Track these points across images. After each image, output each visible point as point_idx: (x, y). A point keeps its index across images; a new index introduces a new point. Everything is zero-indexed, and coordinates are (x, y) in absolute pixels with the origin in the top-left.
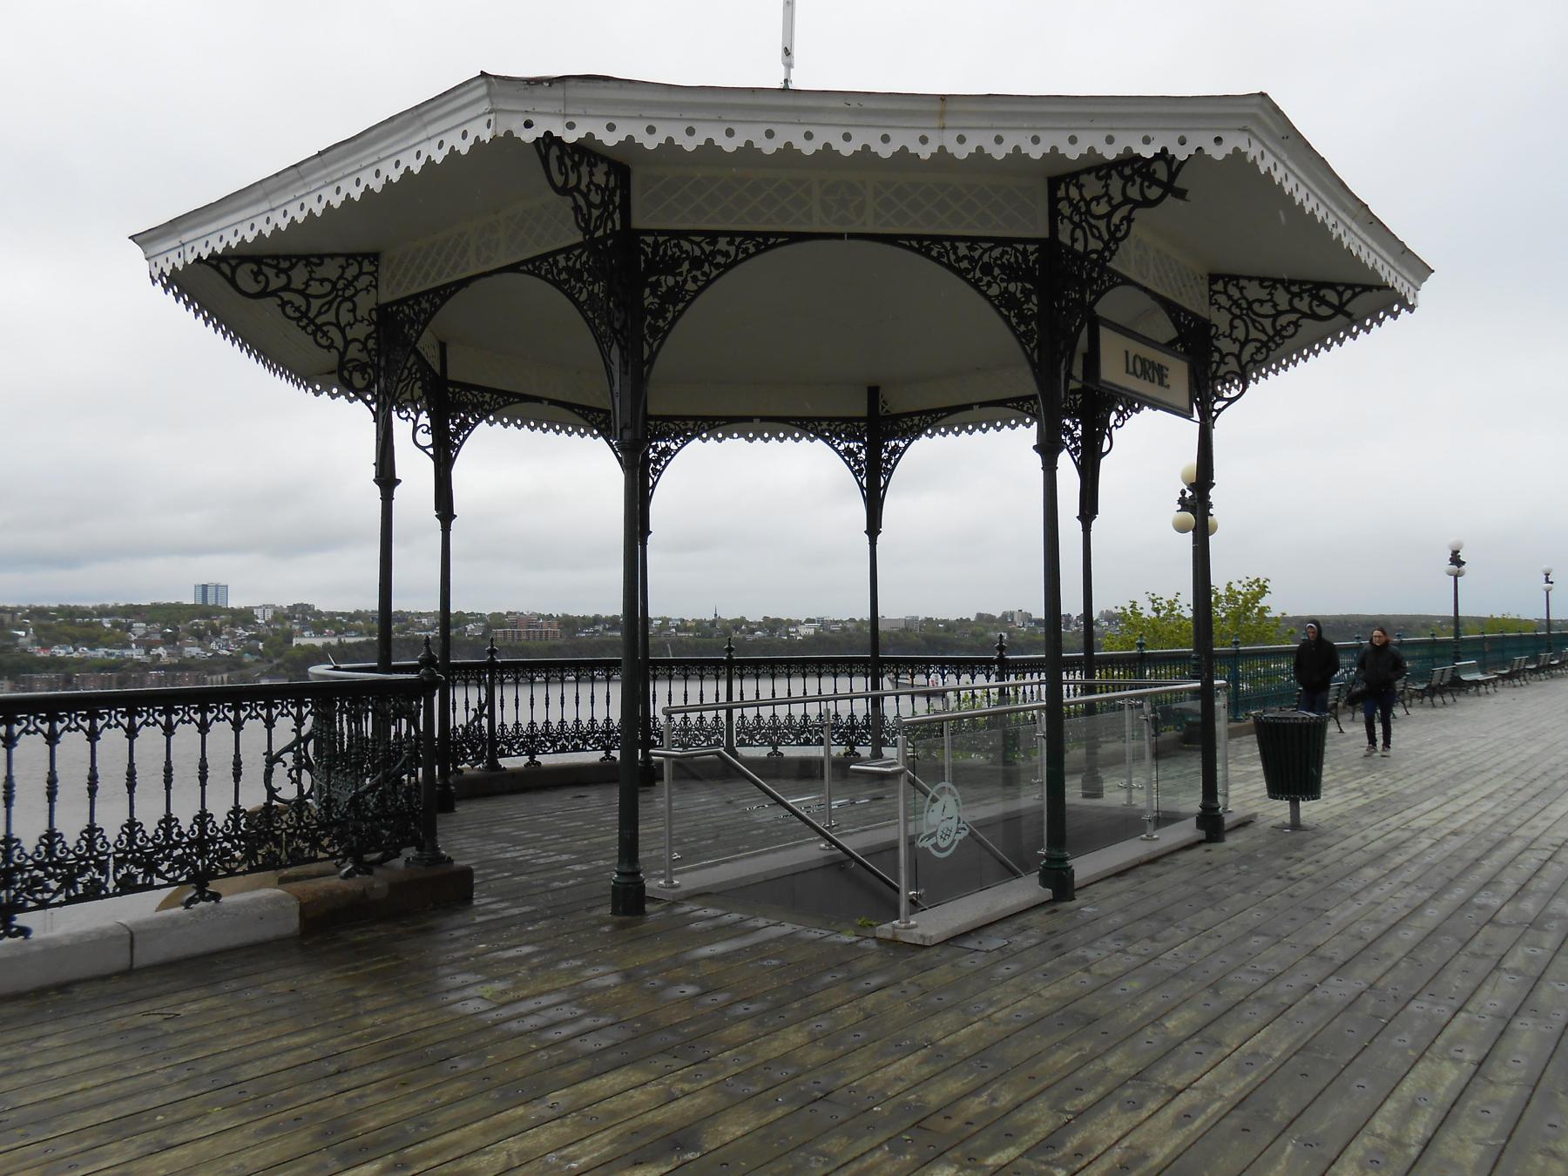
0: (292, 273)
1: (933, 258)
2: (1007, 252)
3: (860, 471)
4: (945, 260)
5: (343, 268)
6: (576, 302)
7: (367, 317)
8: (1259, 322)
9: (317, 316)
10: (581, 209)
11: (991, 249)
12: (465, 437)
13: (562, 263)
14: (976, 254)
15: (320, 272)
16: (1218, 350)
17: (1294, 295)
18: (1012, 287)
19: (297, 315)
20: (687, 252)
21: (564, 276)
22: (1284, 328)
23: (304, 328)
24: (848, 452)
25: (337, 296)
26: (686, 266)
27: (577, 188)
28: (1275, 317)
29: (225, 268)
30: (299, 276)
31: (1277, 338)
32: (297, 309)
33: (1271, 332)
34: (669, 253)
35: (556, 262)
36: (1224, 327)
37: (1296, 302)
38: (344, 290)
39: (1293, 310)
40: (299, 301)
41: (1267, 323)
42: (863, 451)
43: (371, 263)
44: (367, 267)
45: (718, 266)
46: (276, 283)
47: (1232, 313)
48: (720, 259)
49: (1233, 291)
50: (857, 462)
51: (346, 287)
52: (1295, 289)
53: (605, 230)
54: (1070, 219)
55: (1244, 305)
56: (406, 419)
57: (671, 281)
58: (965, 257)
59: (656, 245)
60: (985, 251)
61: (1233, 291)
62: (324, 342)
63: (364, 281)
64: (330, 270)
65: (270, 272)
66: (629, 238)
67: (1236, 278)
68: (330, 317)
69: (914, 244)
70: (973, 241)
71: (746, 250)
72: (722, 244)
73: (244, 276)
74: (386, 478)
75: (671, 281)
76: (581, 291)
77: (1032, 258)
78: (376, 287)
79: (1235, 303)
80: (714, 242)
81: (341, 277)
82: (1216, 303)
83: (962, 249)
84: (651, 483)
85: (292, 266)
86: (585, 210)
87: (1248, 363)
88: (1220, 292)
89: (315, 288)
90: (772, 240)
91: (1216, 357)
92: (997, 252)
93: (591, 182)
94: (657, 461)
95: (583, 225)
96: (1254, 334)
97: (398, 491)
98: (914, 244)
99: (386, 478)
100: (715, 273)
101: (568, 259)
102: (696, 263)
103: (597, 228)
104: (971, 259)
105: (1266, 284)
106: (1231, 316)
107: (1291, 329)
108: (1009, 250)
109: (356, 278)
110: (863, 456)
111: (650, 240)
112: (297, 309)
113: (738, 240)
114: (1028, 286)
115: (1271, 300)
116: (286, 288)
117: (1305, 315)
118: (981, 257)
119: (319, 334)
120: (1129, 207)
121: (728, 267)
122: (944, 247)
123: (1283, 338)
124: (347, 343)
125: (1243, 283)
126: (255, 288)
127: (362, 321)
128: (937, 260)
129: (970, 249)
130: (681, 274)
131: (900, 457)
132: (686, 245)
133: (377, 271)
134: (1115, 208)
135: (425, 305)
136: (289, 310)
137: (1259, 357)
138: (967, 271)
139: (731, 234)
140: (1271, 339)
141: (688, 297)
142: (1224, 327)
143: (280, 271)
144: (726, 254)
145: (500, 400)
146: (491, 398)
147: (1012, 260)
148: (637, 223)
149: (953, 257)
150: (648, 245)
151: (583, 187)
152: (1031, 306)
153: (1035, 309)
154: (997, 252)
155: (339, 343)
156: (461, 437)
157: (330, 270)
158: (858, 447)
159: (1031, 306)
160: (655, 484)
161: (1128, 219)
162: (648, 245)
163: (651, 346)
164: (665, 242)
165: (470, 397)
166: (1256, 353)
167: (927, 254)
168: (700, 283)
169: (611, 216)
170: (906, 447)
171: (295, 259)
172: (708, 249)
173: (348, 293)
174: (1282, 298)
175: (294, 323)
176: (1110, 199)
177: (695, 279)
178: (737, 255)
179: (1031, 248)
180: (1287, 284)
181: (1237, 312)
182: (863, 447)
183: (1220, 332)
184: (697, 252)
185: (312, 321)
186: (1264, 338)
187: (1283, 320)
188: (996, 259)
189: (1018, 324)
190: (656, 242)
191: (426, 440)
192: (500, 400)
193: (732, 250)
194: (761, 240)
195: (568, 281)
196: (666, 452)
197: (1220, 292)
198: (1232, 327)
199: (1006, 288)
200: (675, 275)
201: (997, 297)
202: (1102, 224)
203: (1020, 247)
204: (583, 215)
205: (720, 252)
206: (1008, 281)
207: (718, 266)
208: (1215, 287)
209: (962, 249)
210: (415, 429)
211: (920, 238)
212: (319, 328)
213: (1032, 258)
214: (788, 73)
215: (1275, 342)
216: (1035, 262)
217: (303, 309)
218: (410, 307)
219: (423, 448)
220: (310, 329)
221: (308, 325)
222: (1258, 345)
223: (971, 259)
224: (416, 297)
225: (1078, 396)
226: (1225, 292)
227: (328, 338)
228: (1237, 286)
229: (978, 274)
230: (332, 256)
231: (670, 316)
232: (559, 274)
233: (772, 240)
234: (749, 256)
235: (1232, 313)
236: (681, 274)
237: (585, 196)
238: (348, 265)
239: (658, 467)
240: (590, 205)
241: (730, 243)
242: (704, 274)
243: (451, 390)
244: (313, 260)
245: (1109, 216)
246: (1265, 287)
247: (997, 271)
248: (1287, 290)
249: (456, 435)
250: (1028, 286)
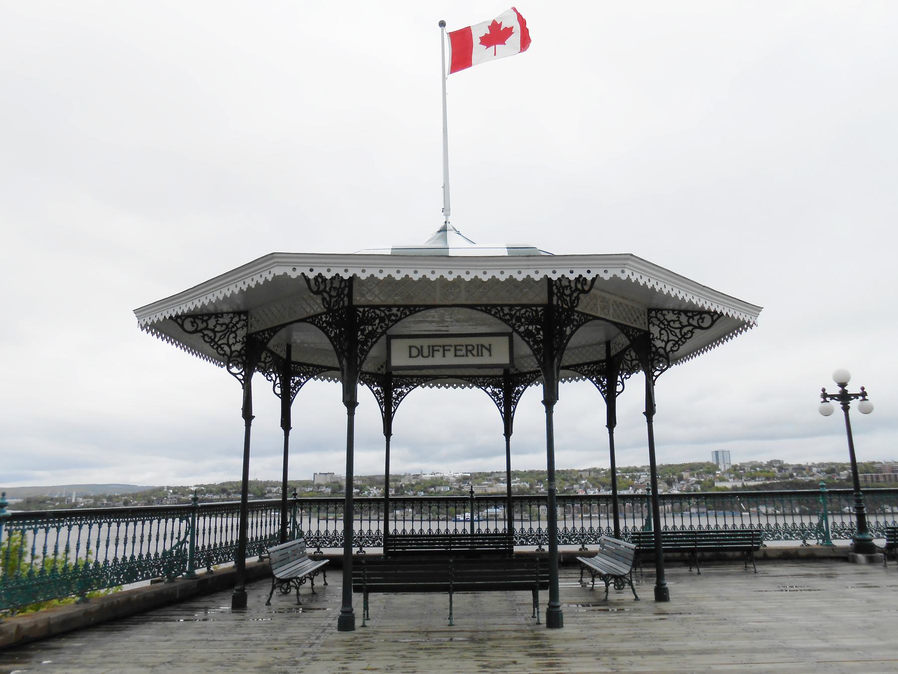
0: (209, 322)
1: (492, 315)
2: (528, 311)
4: (498, 315)
5: (232, 318)
6: (329, 337)
7: (241, 340)
8: (674, 332)
9: (219, 340)
10: (326, 299)
11: (520, 310)
12: (299, 389)
13: (324, 319)
14: (513, 313)
15: (221, 321)
16: (654, 346)
17: (689, 318)
18: (530, 327)
19: (210, 340)
20: (378, 315)
21: (325, 325)
22: (686, 334)
23: (213, 347)
24: (494, 394)
25: (228, 332)
26: (377, 321)
27: (324, 290)
28: (681, 328)
29: (179, 320)
30: (212, 323)
31: (683, 339)
32: (210, 338)
33: (680, 337)
34: (370, 315)
35: (322, 318)
36: (657, 334)
37: (691, 320)
38: (231, 328)
39: (690, 325)
40: (211, 334)
41: (677, 331)
42: (502, 393)
43: (245, 315)
44: (243, 317)
45: (392, 321)
46: (201, 326)
47: (660, 328)
48: (393, 318)
49: (659, 316)
50: (499, 399)
51: (233, 327)
52: (690, 314)
53: (339, 306)
54: (557, 295)
55: (666, 323)
56: (270, 381)
57: (370, 328)
58: (507, 314)
59: (364, 312)
60: (517, 311)
61: (659, 316)
63: (242, 323)
64: (226, 320)
65: (199, 322)
66: (352, 309)
67: (662, 310)
68: (224, 341)
69: (483, 308)
70: (511, 307)
71: (405, 314)
72: (394, 310)
73: (188, 325)
74: (248, 414)
75: (370, 328)
76: (331, 332)
77: (540, 313)
78: (247, 326)
79: (661, 322)
80: (390, 310)
81: (231, 322)
82: (652, 323)
83: (506, 310)
84: (393, 410)
85: (208, 319)
86: (328, 299)
87: (669, 352)
88: (653, 317)
89: (218, 328)
90: (417, 309)
91: (654, 349)
92: (523, 311)
93: (331, 287)
94: (397, 399)
95: (327, 306)
96: (671, 337)
97: (253, 421)
98: (483, 308)
99: (248, 414)
100: (391, 324)
101: (326, 317)
102: (382, 320)
103: (334, 306)
105: (676, 312)
106: (687, 318)
107: (689, 335)
108: (529, 310)
109: (237, 323)
110: (501, 395)
111: (361, 310)
112: (210, 338)
113: (401, 309)
114: (538, 327)
115: (678, 320)
116: (206, 328)
117: (695, 327)
118: (515, 313)
119: (219, 349)
120: (578, 292)
121: (396, 321)
122: (497, 309)
123: (686, 339)
125: (665, 312)
126: (194, 329)
127: (239, 342)
128: (494, 315)
129: (511, 310)
130: (375, 325)
131: (520, 396)
132: (378, 312)
133: (247, 319)
134: (572, 292)
135: (266, 335)
136: (207, 339)
137: (675, 349)
138: (509, 320)
139: (399, 306)
140: (680, 339)
141: (378, 336)
142: (657, 334)
143: (203, 321)
144: (396, 315)
145: (318, 370)
146: (313, 369)
147: (531, 314)
148: (355, 303)
149: (502, 314)
150: (360, 312)
151: (327, 289)
152: (540, 336)
153: (542, 337)
154: (523, 311)
156: (297, 389)
157: (226, 320)
158: (499, 391)
159: (540, 336)
160: (395, 410)
161: (578, 298)
162: (360, 312)
163: (360, 358)
164: (368, 311)
165: (302, 369)
166: (673, 347)
167: (490, 313)
168: (383, 329)
169: (342, 300)
170: (524, 390)
171: (210, 315)
172: (388, 313)
173: (234, 329)
174: (684, 319)
175: (208, 344)
176: (571, 288)
177: (381, 327)
178: (401, 315)
179: (539, 309)
180: (686, 312)
181: (663, 326)
182: (502, 391)
183: (655, 337)
184: (383, 314)
185: (216, 343)
186: (677, 339)
187: (685, 330)
188: (523, 314)
189: (534, 345)
190: (364, 310)
191: (278, 390)
192: (318, 370)
193: (399, 314)
194: (412, 309)
195: (326, 327)
196: (401, 394)
197: (653, 317)
198: (661, 334)
199: (528, 328)
200: (372, 325)
201: (523, 332)
202: (568, 299)
203: (534, 308)
204: (327, 302)
205: (393, 314)
206: (529, 325)
207: (392, 321)
208: (651, 315)
209: (506, 310)
210: (275, 385)
211: (486, 306)
212: (219, 346)
213: (540, 313)
215: (682, 341)
216: (541, 315)
217: (213, 338)
218: (260, 336)
219: (278, 395)
220: (215, 347)
221: (214, 345)
222: (674, 342)
224: (263, 331)
225: (604, 364)
226: (656, 317)
227: (223, 350)
228: (662, 314)
229: (514, 321)
230: (228, 313)
231: (369, 344)
232: (323, 324)
233: (417, 309)
234: (407, 316)
235: (660, 328)
236: (375, 325)
237: (329, 293)
238: (234, 317)
239: (397, 402)
240: (331, 297)
241: (397, 311)
242: (386, 325)
243: (293, 365)
244: (218, 315)
245: (570, 295)
246: (674, 314)
247: (523, 320)
248: (686, 315)
249: (294, 388)
250: (538, 327)
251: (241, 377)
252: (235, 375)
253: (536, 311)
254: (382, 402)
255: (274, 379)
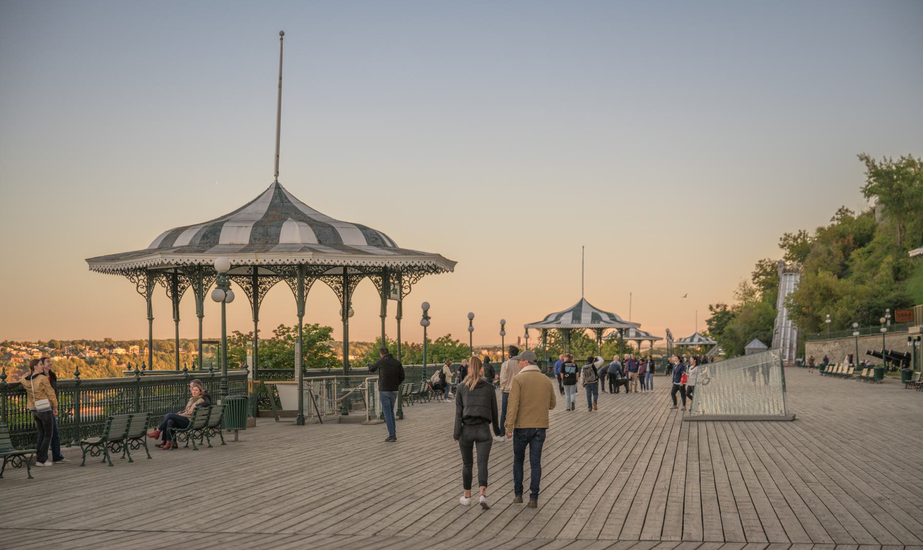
3: (340, 296)
62: (133, 281)
83: (279, 268)
92: (287, 268)
94: (262, 293)
104: (281, 270)
124: (139, 281)
154: (287, 268)
155: (137, 281)
160: (261, 302)
191: (170, 294)
209: (279, 268)
214: (277, 178)
223: (281, 270)
249: (180, 292)
251: (145, 295)
252: (141, 294)
253: (294, 268)
254: (251, 296)
255: (166, 285)
